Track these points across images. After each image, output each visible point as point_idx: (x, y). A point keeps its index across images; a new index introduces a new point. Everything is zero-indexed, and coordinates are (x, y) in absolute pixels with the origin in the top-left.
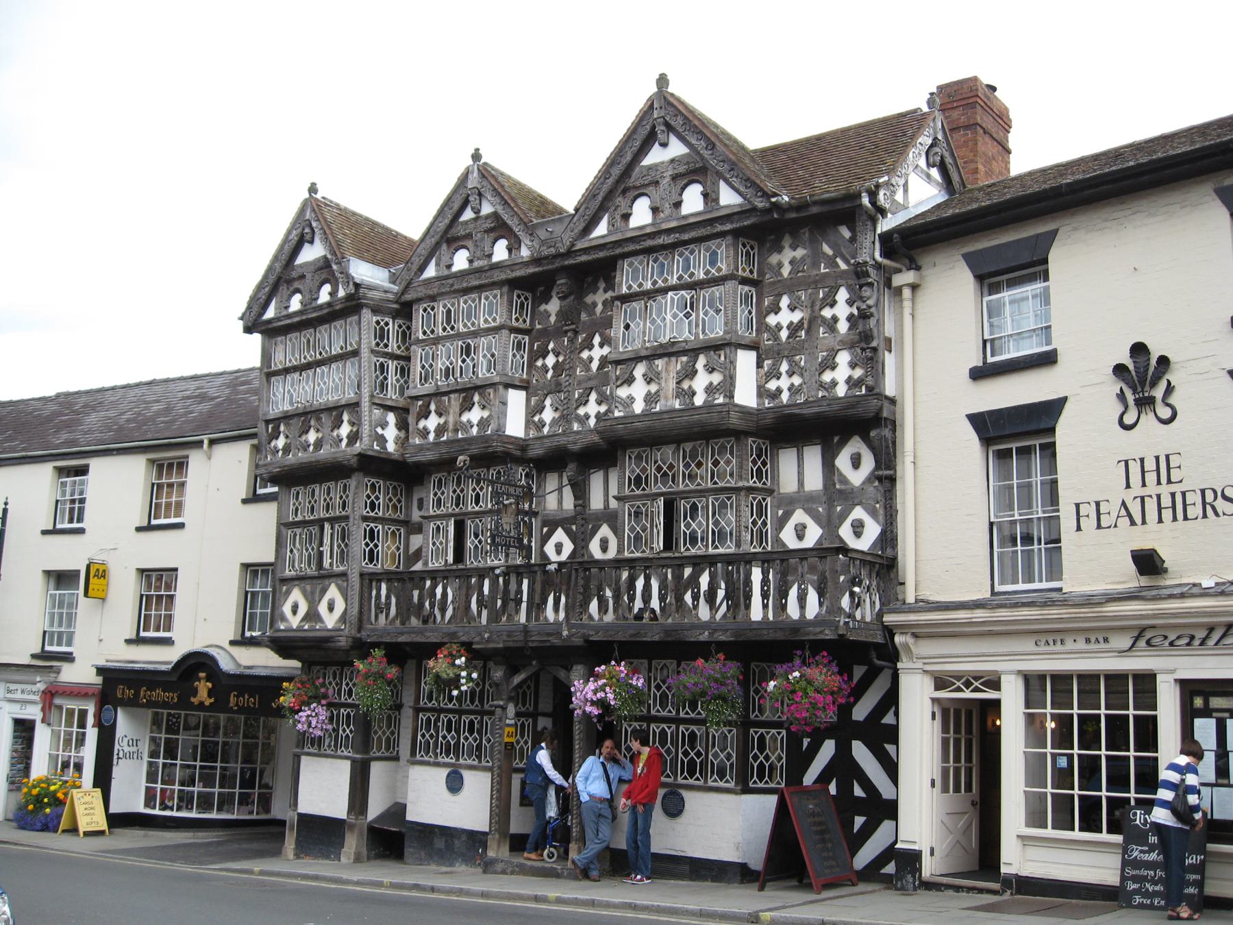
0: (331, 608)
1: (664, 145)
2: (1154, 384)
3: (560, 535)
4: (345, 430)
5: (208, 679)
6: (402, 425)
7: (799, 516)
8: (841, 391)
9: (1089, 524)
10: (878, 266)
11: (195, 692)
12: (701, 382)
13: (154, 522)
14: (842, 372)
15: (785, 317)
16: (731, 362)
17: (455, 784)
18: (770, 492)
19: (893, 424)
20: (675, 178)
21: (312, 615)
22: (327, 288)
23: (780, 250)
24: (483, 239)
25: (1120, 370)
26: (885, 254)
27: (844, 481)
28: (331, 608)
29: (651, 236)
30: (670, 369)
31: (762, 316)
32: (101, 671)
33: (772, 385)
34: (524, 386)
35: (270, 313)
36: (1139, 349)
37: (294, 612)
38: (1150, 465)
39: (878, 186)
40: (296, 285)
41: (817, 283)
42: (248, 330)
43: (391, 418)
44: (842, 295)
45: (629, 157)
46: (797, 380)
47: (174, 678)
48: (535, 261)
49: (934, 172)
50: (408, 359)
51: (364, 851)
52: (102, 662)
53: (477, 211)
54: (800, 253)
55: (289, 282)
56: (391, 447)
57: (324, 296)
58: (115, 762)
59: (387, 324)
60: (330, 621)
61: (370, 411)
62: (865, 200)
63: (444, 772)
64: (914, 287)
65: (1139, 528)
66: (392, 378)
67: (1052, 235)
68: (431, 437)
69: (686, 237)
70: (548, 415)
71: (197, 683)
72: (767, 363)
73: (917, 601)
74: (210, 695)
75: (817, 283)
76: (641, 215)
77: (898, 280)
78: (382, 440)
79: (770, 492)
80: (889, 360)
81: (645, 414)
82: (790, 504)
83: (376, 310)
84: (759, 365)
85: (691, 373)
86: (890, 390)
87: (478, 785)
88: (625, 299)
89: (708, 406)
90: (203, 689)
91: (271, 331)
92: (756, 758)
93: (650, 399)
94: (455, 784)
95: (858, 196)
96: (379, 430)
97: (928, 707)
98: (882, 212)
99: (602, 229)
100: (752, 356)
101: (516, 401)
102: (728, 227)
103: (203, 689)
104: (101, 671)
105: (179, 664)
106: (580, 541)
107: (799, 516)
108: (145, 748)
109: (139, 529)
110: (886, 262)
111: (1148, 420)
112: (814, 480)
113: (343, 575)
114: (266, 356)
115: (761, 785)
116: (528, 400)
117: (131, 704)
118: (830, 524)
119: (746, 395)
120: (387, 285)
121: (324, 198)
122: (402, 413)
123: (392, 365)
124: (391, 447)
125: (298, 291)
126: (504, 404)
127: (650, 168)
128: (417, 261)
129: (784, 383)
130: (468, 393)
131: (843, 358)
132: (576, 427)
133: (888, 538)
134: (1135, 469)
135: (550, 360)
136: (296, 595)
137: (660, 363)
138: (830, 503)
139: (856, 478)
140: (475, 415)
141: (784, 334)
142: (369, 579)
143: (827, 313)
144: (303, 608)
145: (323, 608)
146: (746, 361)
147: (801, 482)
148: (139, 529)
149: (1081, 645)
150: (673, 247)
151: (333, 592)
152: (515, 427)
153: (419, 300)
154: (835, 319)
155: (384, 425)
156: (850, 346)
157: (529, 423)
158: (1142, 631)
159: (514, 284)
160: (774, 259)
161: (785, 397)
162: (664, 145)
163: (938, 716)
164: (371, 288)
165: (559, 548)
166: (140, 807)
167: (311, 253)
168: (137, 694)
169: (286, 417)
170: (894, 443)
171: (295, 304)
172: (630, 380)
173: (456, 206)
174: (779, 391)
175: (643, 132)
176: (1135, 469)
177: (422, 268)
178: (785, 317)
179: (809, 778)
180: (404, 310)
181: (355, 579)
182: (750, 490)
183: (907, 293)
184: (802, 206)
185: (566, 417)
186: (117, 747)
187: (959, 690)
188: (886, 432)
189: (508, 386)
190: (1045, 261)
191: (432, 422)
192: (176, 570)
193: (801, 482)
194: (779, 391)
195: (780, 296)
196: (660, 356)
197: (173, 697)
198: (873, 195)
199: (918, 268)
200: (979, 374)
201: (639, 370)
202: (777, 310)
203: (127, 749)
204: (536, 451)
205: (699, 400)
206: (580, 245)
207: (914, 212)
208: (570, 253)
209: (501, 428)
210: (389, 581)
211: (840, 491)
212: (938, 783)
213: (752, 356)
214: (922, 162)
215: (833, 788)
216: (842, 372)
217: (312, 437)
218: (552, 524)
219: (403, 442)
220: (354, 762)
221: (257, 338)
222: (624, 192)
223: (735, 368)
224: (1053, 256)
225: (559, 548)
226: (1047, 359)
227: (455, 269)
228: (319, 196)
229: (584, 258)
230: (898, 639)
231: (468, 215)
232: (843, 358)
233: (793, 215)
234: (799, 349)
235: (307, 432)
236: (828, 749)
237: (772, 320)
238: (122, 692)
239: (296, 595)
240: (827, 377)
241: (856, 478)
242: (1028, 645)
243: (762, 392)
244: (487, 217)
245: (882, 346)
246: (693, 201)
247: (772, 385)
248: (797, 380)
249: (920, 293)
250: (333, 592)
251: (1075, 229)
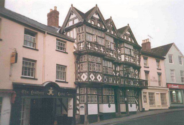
0: (99, 78)
1: (128, 32)
3: (114, 73)
17: (109, 106)
21: (96, 79)
28: (99, 78)
37: (92, 78)
40: (93, 20)
60: (99, 80)
63: (108, 104)
71: (49, 90)
74: (53, 93)
87: (113, 106)
90: (51, 92)
94: (109, 106)
103: (51, 92)
131: (138, 62)
136: (92, 75)
139: (137, 73)
144: (94, 77)
145: (98, 78)
151: (99, 76)
156: (138, 61)
162: (128, 32)
169: (91, 43)
192: (35, 61)
216: (138, 63)
226: (148, 67)
241: (137, 73)
244: (112, 27)
250: (99, 76)
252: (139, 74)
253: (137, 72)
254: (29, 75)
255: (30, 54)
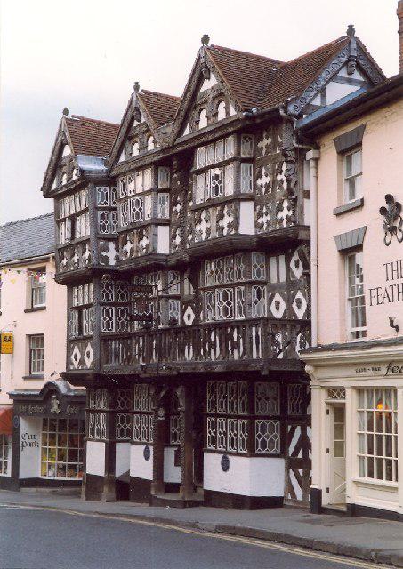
1: (209, 79)
2: (395, 219)
3: (189, 310)
4: (87, 254)
5: (57, 399)
6: (117, 250)
7: (278, 297)
8: (285, 224)
9: (374, 301)
10: (295, 149)
11: (52, 406)
12: (227, 220)
13: (35, 306)
14: (285, 213)
15: (264, 181)
16: (237, 210)
18: (265, 283)
19: (308, 242)
20: (214, 99)
21: (82, 362)
22: (75, 171)
23: (261, 139)
24: (143, 137)
25: (383, 211)
26: (297, 143)
27: (294, 276)
29: (203, 135)
30: (214, 213)
31: (255, 180)
32: (11, 396)
33: (260, 221)
34: (167, 223)
35: (54, 187)
36: (389, 198)
38: (395, 264)
39: (287, 103)
41: (274, 159)
42: (47, 196)
43: (112, 245)
44: (285, 167)
45: (193, 88)
46: (269, 218)
47: (41, 399)
48: (163, 151)
49: (357, 76)
50: (115, 209)
51: (114, 495)
52: (12, 390)
53: (139, 121)
54: (270, 140)
55: (61, 167)
56: (112, 262)
57: (74, 178)
58: (21, 449)
59: (105, 190)
60: (89, 362)
61: (97, 244)
62: (282, 112)
63: (144, 447)
64: (317, 160)
65: (392, 303)
66: (110, 221)
67: (362, 130)
68: (129, 254)
69: (217, 135)
70: (178, 240)
72: (258, 207)
73: (318, 345)
74: (59, 406)
75: (274, 159)
76: (203, 123)
77: (310, 155)
78: (107, 258)
79: (265, 283)
80: (309, 206)
81: (206, 239)
82: (273, 289)
83: (97, 183)
84: (255, 210)
85: (221, 217)
86: (308, 219)
88: (198, 172)
89: (229, 235)
90: (55, 403)
91: (58, 197)
92: (259, 436)
93: (208, 231)
95: (277, 110)
96: (104, 254)
97: (324, 408)
98: (299, 117)
99: (187, 131)
100: (252, 203)
101: (163, 232)
102: (232, 129)
103: (55, 403)
104: (11, 396)
105: (42, 391)
106: (197, 311)
107: (278, 297)
108: (39, 440)
109: (26, 311)
110: (301, 146)
111: (394, 238)
112: (283, 278)
113: (91, 337)
114: (57, 212)
115: (263, 452)
116: (170, 231)
117: (25, 414)
118: (289, 301)
119: (247, 227)
120: (103, 168)
121: (73, 116)
122: (115, 239)
123: (110, 214)
124: (112, 262)
125: (64, 173)
126: (156, 235)
127: (203, 92)
128: (115, 151)
129: (264, 220)
130: (140, 229)
131: (286, 204)
132: (188, 246)
133: (308, 312)
134: (389, 266)
135: (178, 207)
136: (76, 350)
137: (210, 210)
138: (289, 292)
139: (298, 273)
140: (144, 242)
141: (264, 190)
142: (105, 340)
143: (279, 178)
146: (247, 209)
147: (278, 278)
148: (26, 311)
149: (370, 372)
150: (214, 141)
151: (89, 349)
152: (163, 248)
153: (118, 176)
154: (282, 181)
155: (107, 250)
157: (170, 244)
158: (391, 363)
159: (156, 166)
160: (260, 145)
161: (265, 225)
162: (209, 79)
163: (331, 412)
164: (90, 172)
165: (189, 316)
166: (37, 474)
167: (67, 151)
168: (27, 409)
169: (65, 248)
170: (309, 254)
171: (64, 182)
172: (200, 221)
173: (129, 118)
174: (262, 224)
175: (197, 74)
176: (389, 266)
177: (118, 156)
178: (264, 181)
179: (291, 449)
180: (110, 180)
181: (96, 339)
182: (252, 283)
183: (312, 163)
184: (261, 116)
185: (183, 243)
186: (21, 440)
187: (335, 397)
188: (303, 247)
189: (158, 223)
190: (360, 144)
191: (128, 247)
192: (43, 334)
193: (278, 278)
194: (262, 224)
195: (261, 168)
196: (210, 207)
197: (42, 409)
198: (285, 108)
199: (318, 148)
200: (340, 214)
201: (203, 216)
202: (260, 176)
203: (28, 441)
204: (172, 262)
205: (225, 232)
206: (180, 140)
207: (332, 108)
208: (174, 147)
209: (155, 250)
210: (119, 339)
211: (292, 282)
212: (332, 452)
213: (252, 203)
214: (343, 73)
215: (300, 456)
217: (76, 258)
218: (186, 304)
219: (117, 258)
220: (106, 443)
221: (51, 201)
222: (195, 108)
223: (239, 213)
224: (367, 141)
225: (189, 316)
227: (133, 155)
228: (69, 116)
229: (180, 149)
230: (307, 368)
231: (136, 123)
232: (286, 204)
233: (258, 121)
234: (269, 200)
235: (73, 256)
236: (298, 432)
237: (259, 182)
238: (22, 408)
239: (76, 350)
240: (279, 216)
242: (351, 372)
243: (258, 226)
245: (300, 196)
246: (222, 116)
247: (260, 221)
248: (269, 218)
249: (320, 163)
251: (372, 123)
252: (307, 275)
253: (297, 267)
254: (39, 370)
255: (35, 324)
